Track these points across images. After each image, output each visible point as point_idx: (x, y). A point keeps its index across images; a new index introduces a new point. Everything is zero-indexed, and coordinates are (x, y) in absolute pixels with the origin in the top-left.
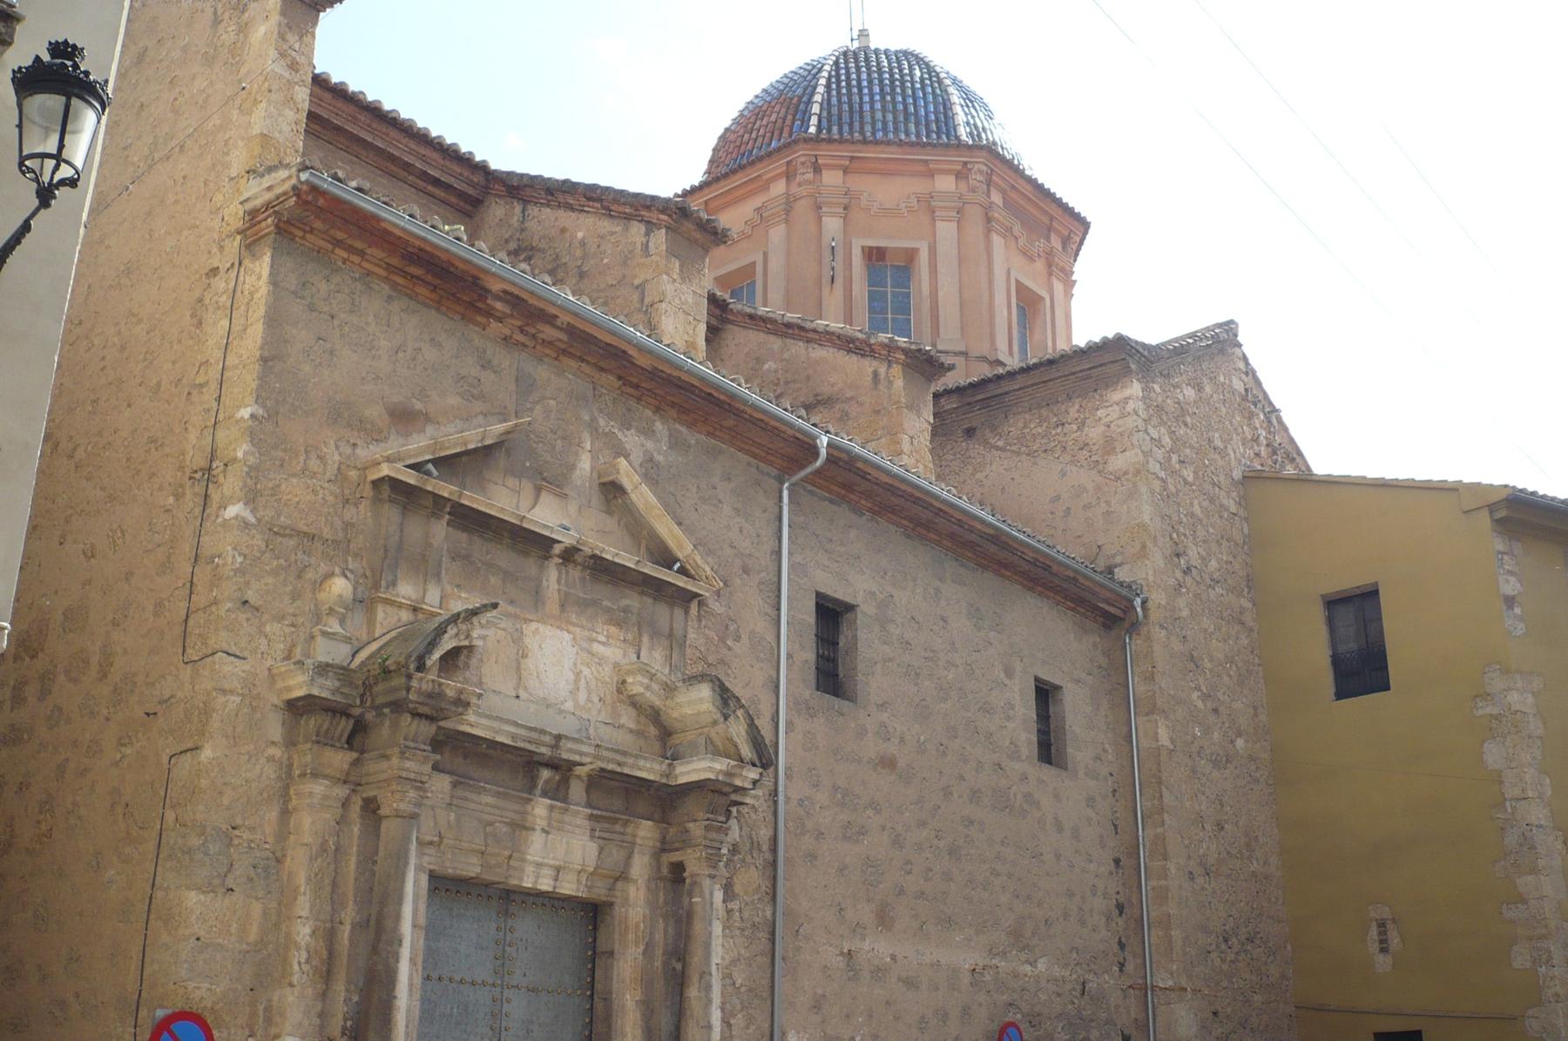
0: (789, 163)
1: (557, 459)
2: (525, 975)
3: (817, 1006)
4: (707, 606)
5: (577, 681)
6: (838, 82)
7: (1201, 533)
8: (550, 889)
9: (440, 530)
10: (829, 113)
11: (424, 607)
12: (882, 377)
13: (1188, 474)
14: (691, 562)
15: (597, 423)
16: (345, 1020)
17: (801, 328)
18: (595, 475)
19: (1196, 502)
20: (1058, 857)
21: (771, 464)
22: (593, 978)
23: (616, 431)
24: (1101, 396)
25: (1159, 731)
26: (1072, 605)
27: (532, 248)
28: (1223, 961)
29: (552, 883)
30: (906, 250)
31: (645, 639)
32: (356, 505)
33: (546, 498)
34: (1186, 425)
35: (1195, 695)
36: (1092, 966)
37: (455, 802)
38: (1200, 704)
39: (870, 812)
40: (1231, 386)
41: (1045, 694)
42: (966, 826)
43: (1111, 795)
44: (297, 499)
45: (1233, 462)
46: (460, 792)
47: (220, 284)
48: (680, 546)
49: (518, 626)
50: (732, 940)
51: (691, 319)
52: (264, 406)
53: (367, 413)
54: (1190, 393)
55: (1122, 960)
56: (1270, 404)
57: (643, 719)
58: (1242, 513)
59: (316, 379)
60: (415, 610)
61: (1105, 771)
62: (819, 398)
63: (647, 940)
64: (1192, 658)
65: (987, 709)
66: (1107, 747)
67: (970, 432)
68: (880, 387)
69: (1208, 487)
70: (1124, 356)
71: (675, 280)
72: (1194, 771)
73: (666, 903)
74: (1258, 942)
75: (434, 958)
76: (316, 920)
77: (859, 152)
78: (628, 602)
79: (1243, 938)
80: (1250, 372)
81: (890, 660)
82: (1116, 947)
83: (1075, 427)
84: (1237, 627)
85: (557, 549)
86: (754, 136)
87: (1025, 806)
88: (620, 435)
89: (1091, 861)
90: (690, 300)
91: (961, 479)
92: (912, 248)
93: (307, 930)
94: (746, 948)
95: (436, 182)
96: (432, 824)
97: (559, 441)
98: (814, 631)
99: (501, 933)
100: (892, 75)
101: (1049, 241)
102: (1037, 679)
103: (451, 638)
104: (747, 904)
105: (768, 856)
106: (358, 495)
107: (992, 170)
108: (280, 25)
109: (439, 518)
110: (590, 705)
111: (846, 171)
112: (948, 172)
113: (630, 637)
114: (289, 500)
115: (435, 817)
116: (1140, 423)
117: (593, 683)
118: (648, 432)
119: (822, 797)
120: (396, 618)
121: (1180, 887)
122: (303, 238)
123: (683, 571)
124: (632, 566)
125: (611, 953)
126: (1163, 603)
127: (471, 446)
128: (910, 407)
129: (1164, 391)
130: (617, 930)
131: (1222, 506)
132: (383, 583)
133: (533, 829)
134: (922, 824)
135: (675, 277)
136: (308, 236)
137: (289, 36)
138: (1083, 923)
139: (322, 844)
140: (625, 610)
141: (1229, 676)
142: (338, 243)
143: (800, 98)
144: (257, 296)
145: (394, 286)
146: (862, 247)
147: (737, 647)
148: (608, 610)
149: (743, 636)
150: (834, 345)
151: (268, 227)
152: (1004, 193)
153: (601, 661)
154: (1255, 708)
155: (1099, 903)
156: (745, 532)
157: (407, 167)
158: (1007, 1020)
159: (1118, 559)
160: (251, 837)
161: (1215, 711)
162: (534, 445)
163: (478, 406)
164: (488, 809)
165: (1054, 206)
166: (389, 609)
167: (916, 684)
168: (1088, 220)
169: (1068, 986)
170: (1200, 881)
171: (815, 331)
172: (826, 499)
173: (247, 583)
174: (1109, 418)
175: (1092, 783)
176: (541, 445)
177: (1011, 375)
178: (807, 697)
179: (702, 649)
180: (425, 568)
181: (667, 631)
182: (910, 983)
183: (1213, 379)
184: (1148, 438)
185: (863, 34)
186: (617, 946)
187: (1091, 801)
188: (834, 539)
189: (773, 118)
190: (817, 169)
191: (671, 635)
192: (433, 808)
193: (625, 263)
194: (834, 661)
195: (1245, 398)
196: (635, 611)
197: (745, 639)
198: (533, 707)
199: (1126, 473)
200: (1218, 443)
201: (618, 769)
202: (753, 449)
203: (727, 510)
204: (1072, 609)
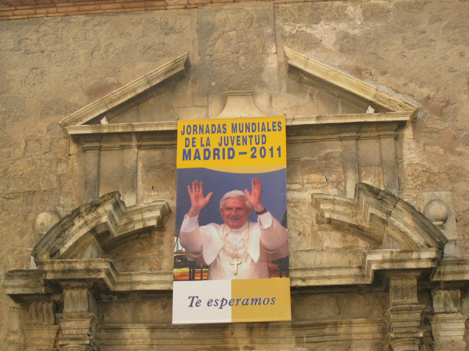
1: (242, 70)
4: (426, 127)
23: (304, 29)
33: (231, 101)
44: (21, 173)
46: (158, 334)
48: (365, 91)
53: (71, 100)
59: (31, 94)
88: (308, 31)
97: (242, 58)
103: (80, 228)
106: (67, 155)
114: (15, 175)
122: (14, 15)
123: (378, 109)
124: (313, 122)
127: (139, 91)
136: (16, 12)
162: (218, 68)
176: (224, 66)
179: (425, 163)
201: (304, 284)
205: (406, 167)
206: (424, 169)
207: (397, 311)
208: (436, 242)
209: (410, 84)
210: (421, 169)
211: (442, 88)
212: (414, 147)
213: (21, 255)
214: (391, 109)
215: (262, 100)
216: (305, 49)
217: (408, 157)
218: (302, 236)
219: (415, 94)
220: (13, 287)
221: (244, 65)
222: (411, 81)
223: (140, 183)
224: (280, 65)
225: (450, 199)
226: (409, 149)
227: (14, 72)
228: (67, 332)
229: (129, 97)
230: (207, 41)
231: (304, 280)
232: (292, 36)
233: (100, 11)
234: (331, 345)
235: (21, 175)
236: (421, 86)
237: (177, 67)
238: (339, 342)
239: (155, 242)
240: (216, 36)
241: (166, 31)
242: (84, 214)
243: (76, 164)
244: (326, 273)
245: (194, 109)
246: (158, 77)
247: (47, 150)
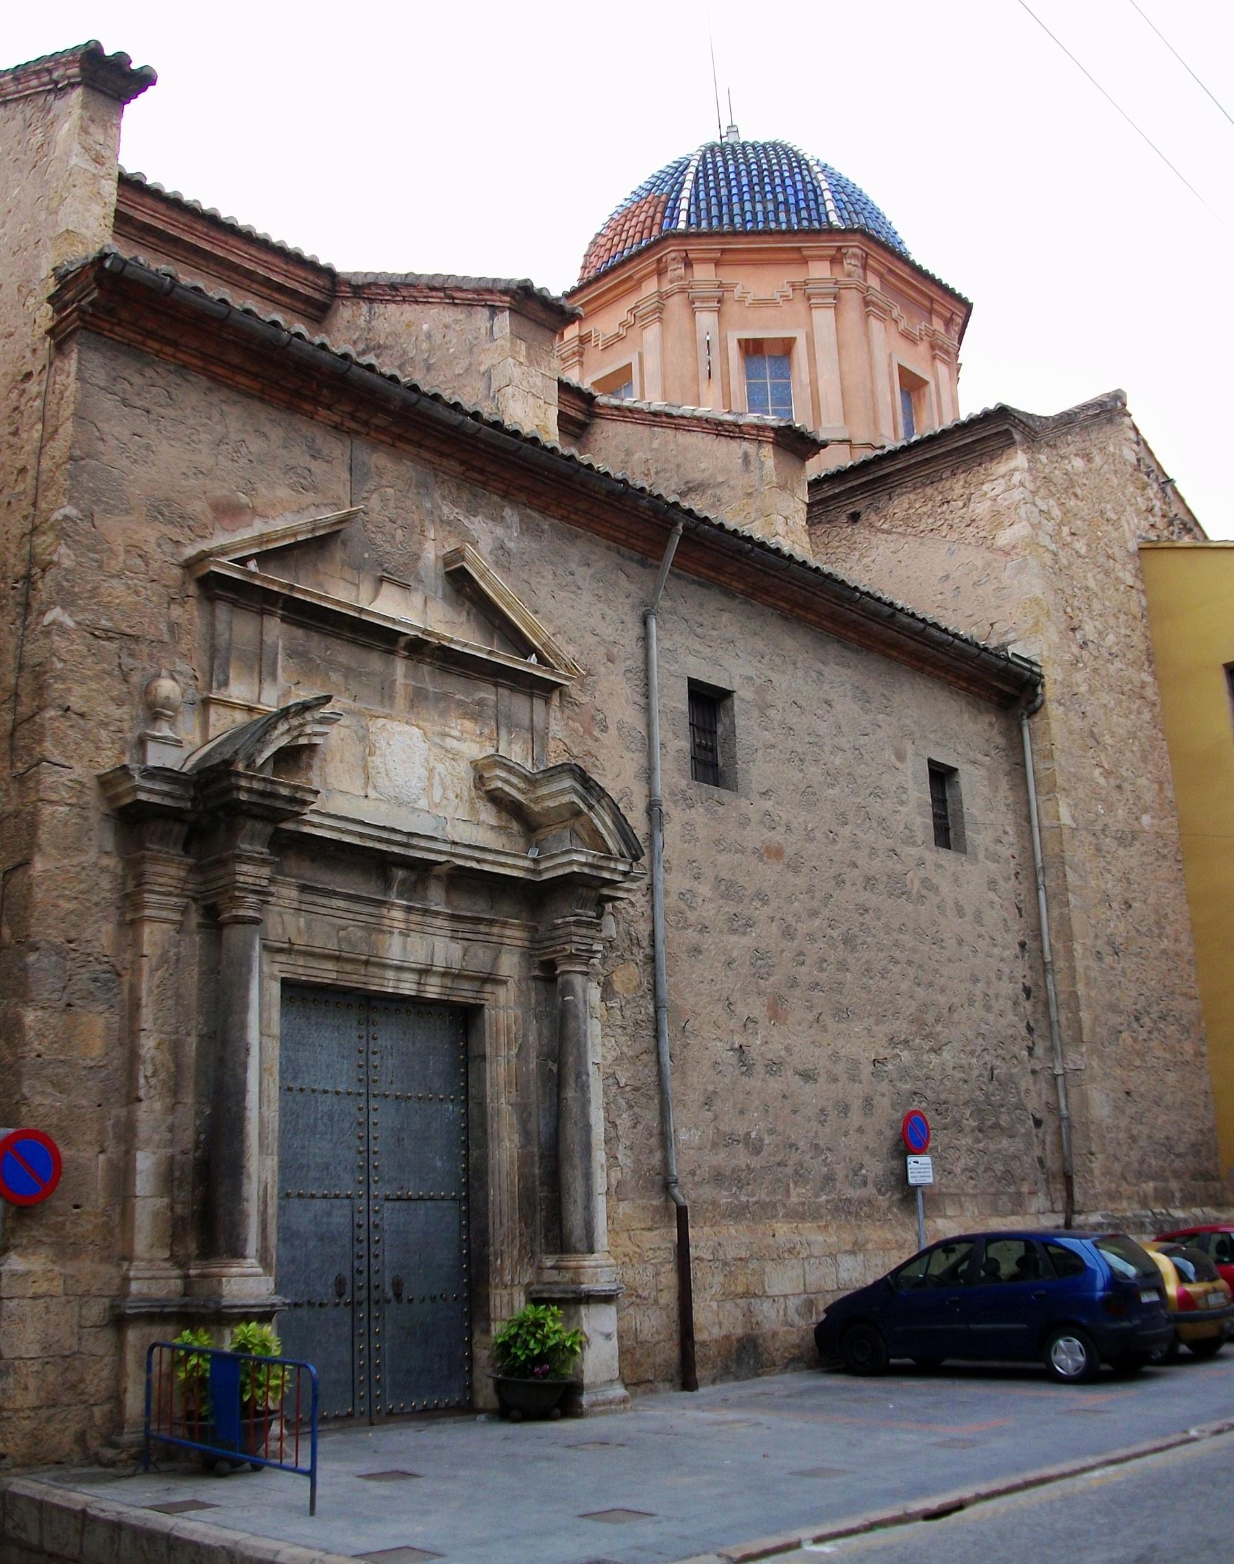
0: (660, 260)
3: (708, 1103)
5: (430, 778)
6: (706, 176)
7: (1096, 606)
8: (413, 993)
9: (275, 630)
10: (698, 207)
11: (260, 706)
12: (752, 459)
13: (1080, 546)
15: (441, 510)
16: (198, 1133)
17: (669, 416)
18: (440, 564)
19: (1090, 575)
20: (960, 942)
21: (632, 547)
22: (467, 1083)
24: (986, 469)
25: (1061, 809)
26: (965, 685)
27: (379, 346)
28: (1135, 1040)
29: (414, 986)
30: (784, 339)
31: (503, 732)
33: (386, 589)
34: (1076, 496)
35: (1098, 771)
36: (1000, 1052)
37: (304, 907)
38: (1102, 781)
39: (757, 903)
40: (1121, 456)
41: (941, 776)
42: (862, 914)
43: (1013, 878)
45: (1128, 534)
47: (33, 387)
49: (364, 723)
50: (613, 1040)
51: (541, 402)
52: (77, 506)
53: (189, 509)
54: (1078, 463)
55: (1030, 1044)
56: (1164, 474)
57: (504, 815)
58: (1139, 585)
60: (250, 709)
61: (1006, 852)
62: (691, 485)
63: (520, 1041)
64: (1092, 734)
65: (878, 793)
66: (1008, 829)
67: (855, 517)
68: (752, 468)
69: (1101, 559)
70: (1006, 427)
71: (521, 363)
72: (1098, 850)
73: (538, 1003)
74: (1170, 1019)
76: (162, 1032)
77: (729, 243)
78: (483, 695)
79: (1155, 1016)
80: (1141, 442)
81: (773, 746)
82: (1024, 1032)
83: (961, 504)
84: (1138, 702)
85: (402, 641)
86: (624, 236)
87: (924, 892)
88: (466, 522)
89: (995, 945)
90: (539, 384)
91: (848, 566)
92: (790, 338)
94: (628, 1046)
95: (281, 288)
96: (280, 931)
97: (399, 531)
98: (687, 721)
99: (364, 1041)
100: (760, 166)
101: (931, 322)
102: (931, 762)
103: (283, 734)
104: (628, 1002)
105: (648, 951)
107: (867, 254)
108: (82, 118)
110: (445, 802)
111: (718, 263)
112: (821, 258)
113: (486, 731)
115: (283, 923)
116: (1027, 494)
117: (448, 781)
118: (499, 519)
119: (705, 890)
120: (230, 719)
121: (1087, 968)
122: (111, 331)
123: (542, 660)
125: (483, 1057)
126: (1059, 678)
127: (300, 538)
128: (782, 487)
129: (1051, 462)
130: (487, 1034)
131: (1117, 579)
132: (215, 684)
134: (814, 914)
135: (522, 360)
136: (117, 329)
137: (92, 129)
138: (988, 1008)
139: (162, 955)
140: (481, 703)
141: (1132, 751)
142: (149, 334)
143: (669, 195)
144: (67, 394)
146: (739, 341)
147: (603, 737)
148: (460, 703)
149: (610, 726)
150: (704, 431)
151: (75, 321)
152: (881, 276)
153: (455, 756)
154: (1161, 783)
155: (1007, 988)
156: (608, 618)
157: (249, 275)
158: (911, 1109)
159: (1011, 636)
160: (88, 951)
161: (1119, 787)
163: (310, 497)
164: (339, 913)
165: (934, 288)
166: (222, 710)
167: (801, 771)
168: (970, 301)
169: (976, 1073)
170: (1109, 960)
171: (683, 417)
172: (694, 582)
173: (69, 690)
174: (995, 492)
175: (993, 866)
177: (893, 455)
178: (685, 788)
180: (262, 666)
181: (527, 722)
182: (807, 1076)
183: (1102, 450)
184: (1036, 510)
185: (733, 129)
186: (488, 1050)
187: (992, 885)
188: (705, 623)
189: (642, 218)
190: (688, 264)
191: (532, 729)
192: (280, 914)
193: (471, 352)
194: (713, 750)
195: (1137, 468)
196: (491, 703)
197: (613, 730)
198: (383, 807)
199: (1014, 547)
200: (1111, 515)
202: (612, 532)
203: (586, 597)
204: (966, 689)
207: (578, 924)
208: (631, 854)
213: (120, 735)
215: (417, 599)
220: (150, 791)
223: (280, 671)
228: (241, 879)
229: (287, 542)
231: (479, 861)
232: (449, 523)
239: (303, 765)
244: (503, 859)
245: (342, 584)
246: (324, 527)
247: (156, 578)
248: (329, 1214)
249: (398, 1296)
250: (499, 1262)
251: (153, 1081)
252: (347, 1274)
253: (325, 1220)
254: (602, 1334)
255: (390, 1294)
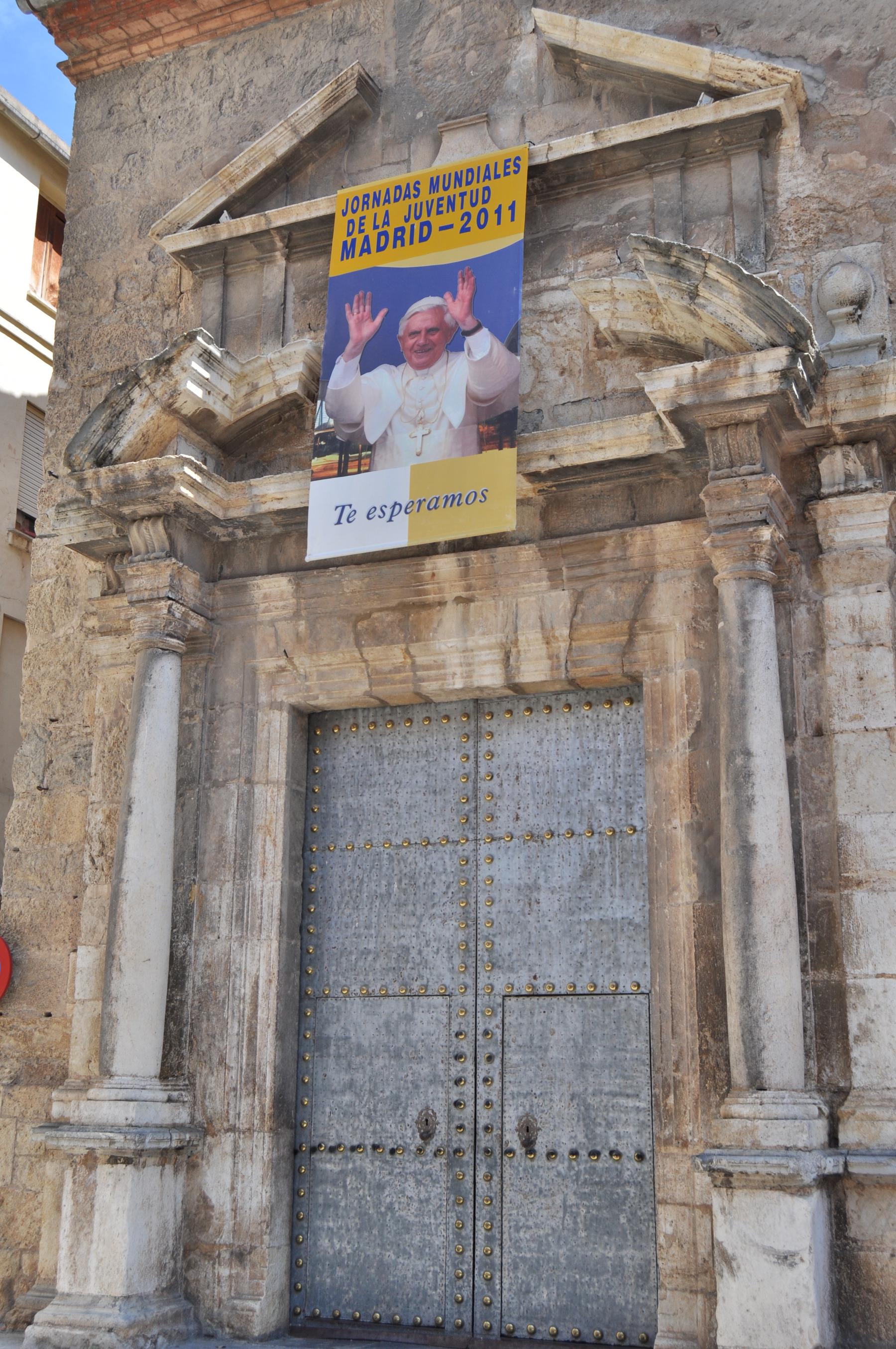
1: (470, 78)
2: (517, 818)
14: (722, 73)
32: (177, 306)
63: (697, 718)
75: (355, 819)
93: (100, 817)
109: (271, 261)
115: (276, 634)
123: (720, 95)
133: (442, 603)
136: (100, 60)
145: (213, 34)
176: (439, 77)
179: (825, 192)
205: (784, 206)
206: (823, 205)
209: (799, 34)
210: (815, 206)
211: (869, 29)
212: (801, 162)
214: (744, 89)
216: (590, 12)
217: (789, 185)
218: (566, 374)
219: (809, 54)
221: (474, 68)
222: (802, 29)
224: (541, 54)
225: (876, 258)
226: (791, 169)
227: (100, 166)
230: (410, 37)
233: (233, 27)
234: (614, 582)
235: (109, 342)
236: (822, 35)
237: (344, 93)
238: (631, 574)
240: (427, 24)
241: (342, 35)
242: (148, 380)
243: (191, 307)
248: (409, 1019)
249: (529, 1145)
250: (671, 1100)
251: (100, 861)
252: (440, 1110)
253: (402, 1027)
254: (768, 1251)
255: (513, 1140)
